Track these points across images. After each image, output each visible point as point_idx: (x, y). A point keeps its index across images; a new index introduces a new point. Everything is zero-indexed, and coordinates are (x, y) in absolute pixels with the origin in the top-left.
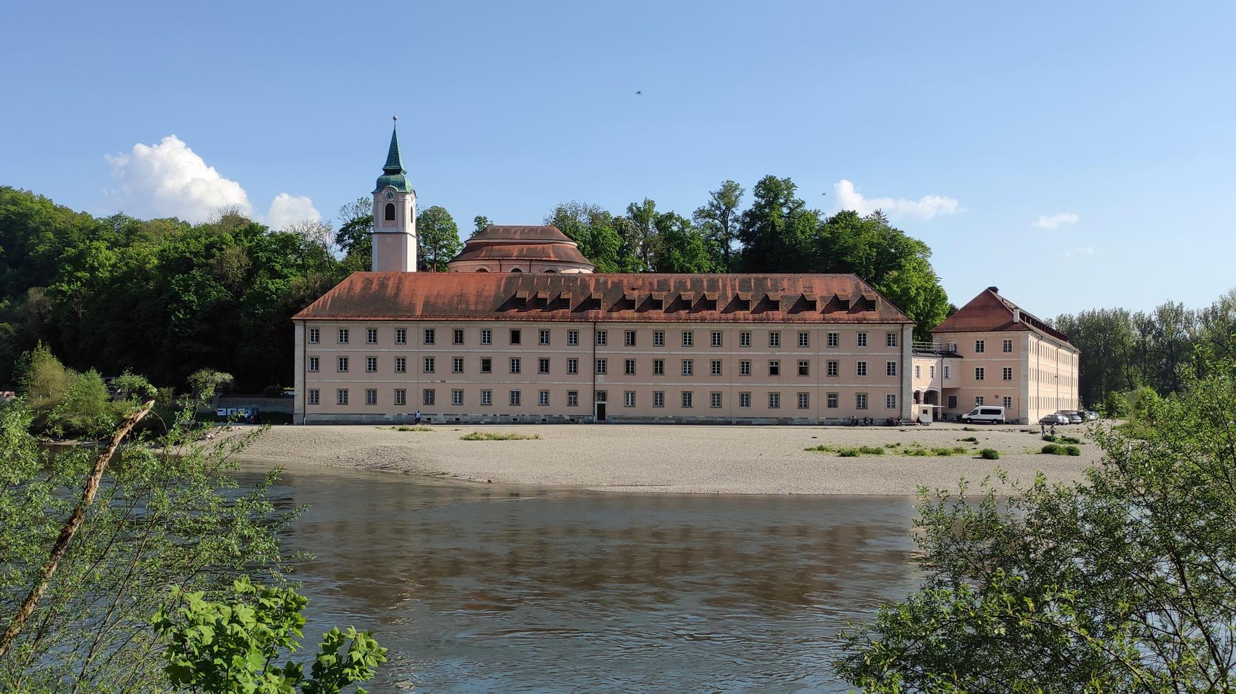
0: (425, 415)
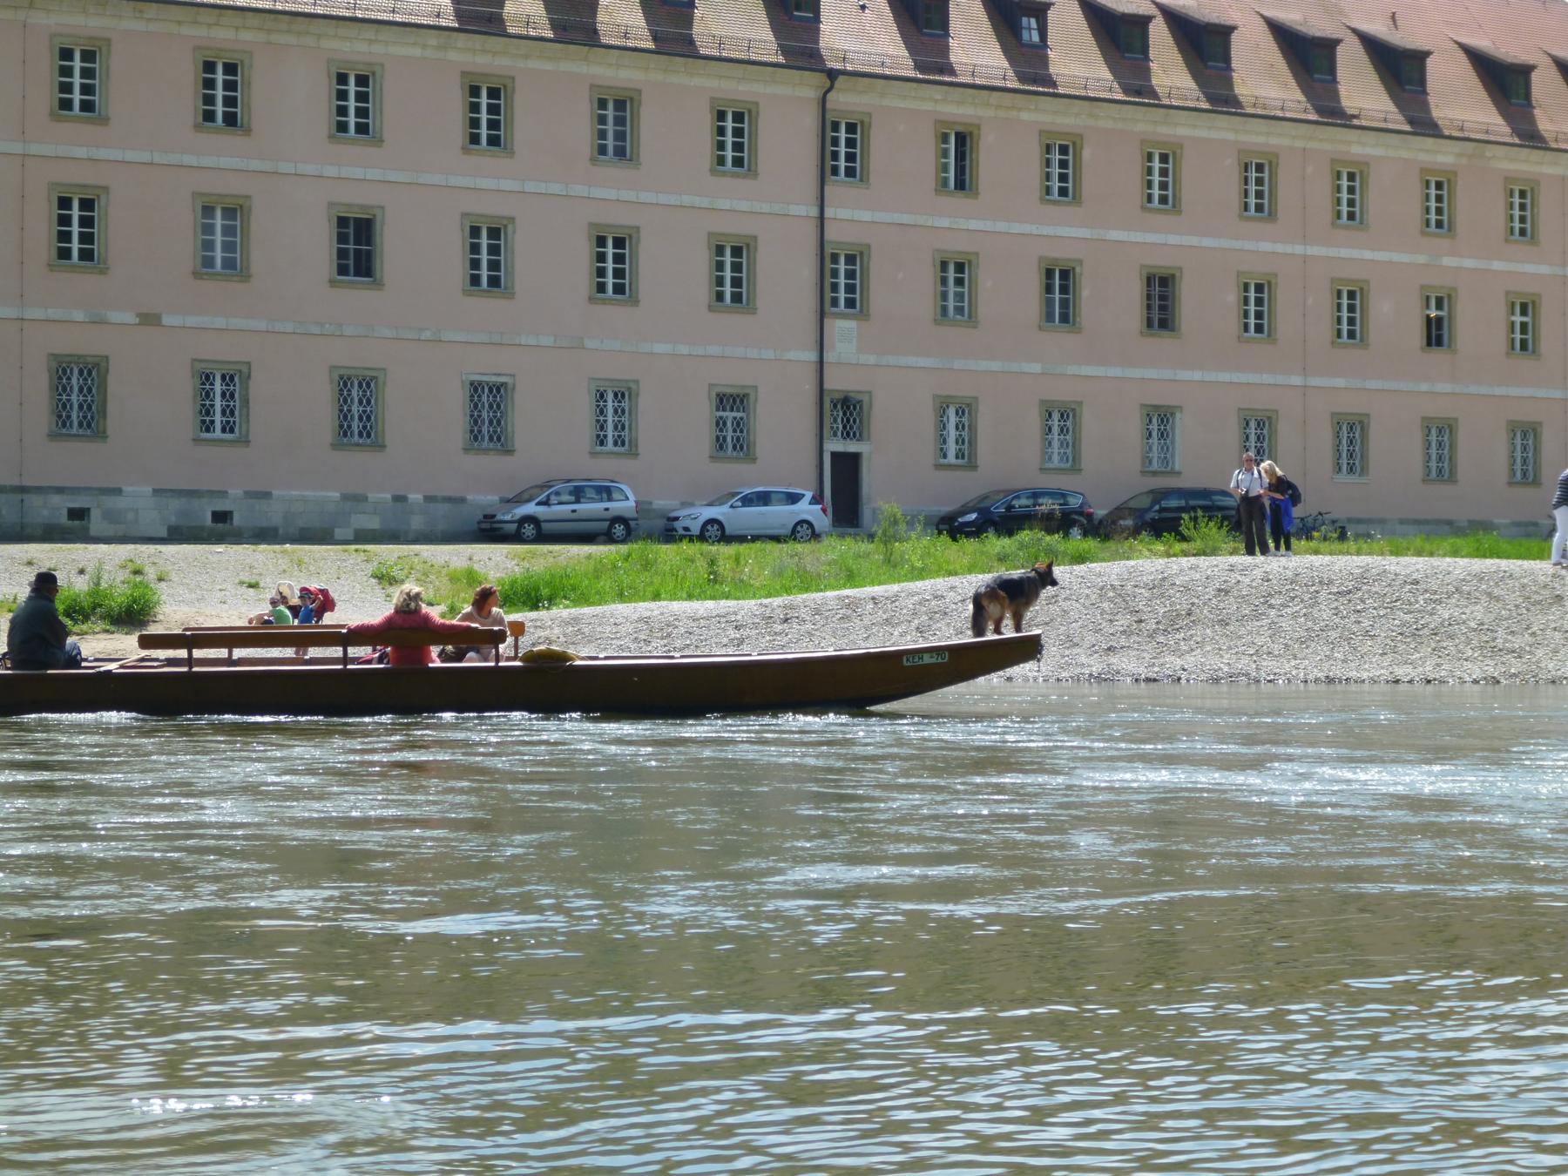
0: (60, 490)
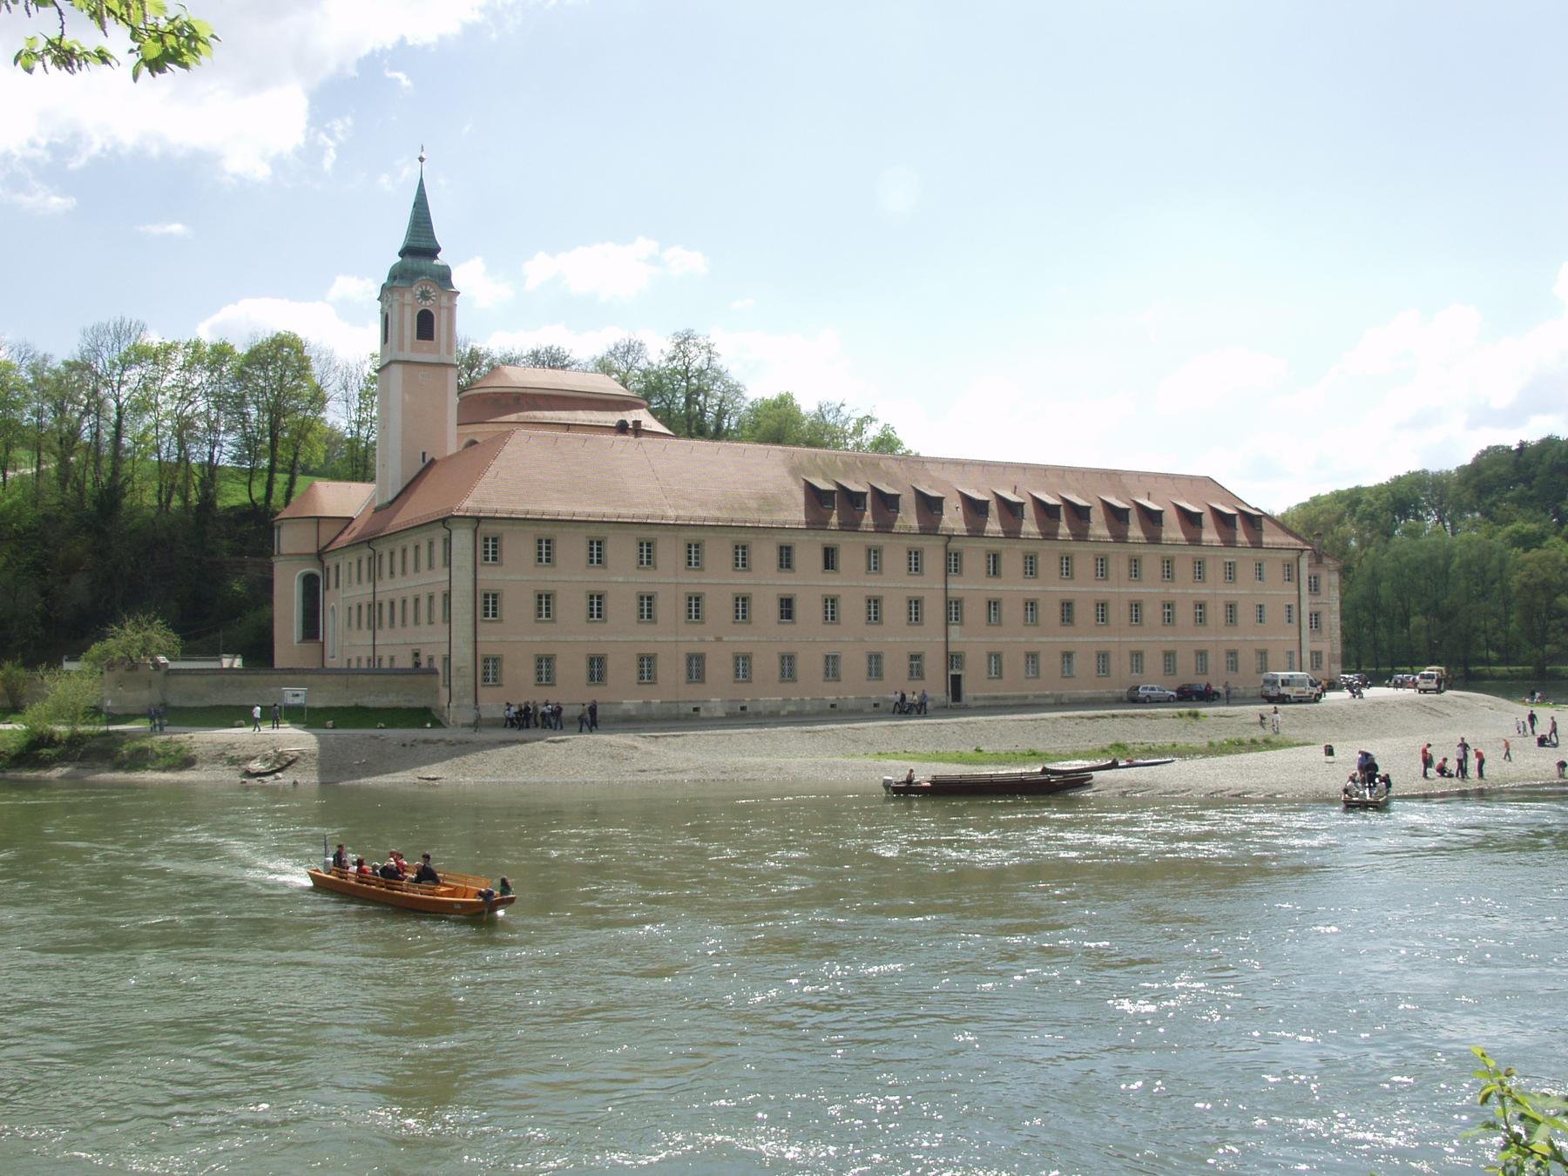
0: (690, 701)
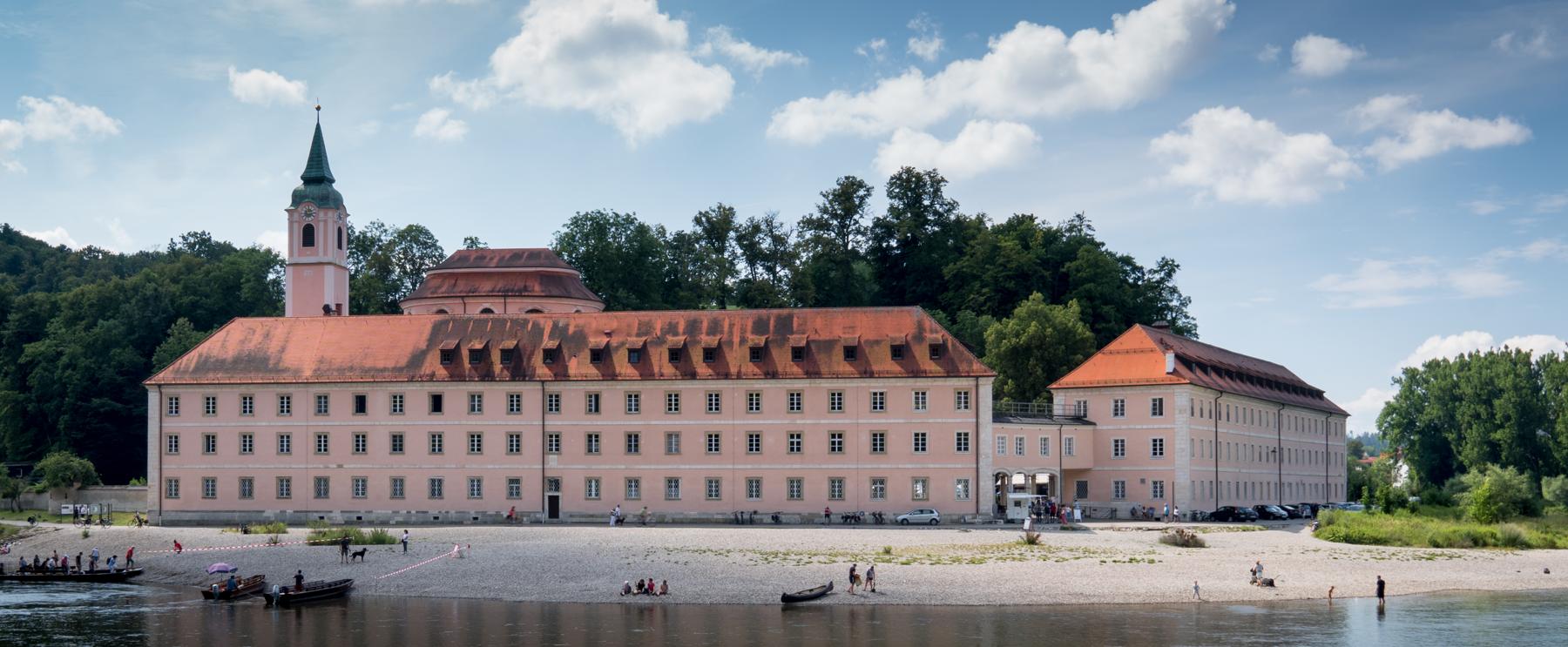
0: (316, 512)
